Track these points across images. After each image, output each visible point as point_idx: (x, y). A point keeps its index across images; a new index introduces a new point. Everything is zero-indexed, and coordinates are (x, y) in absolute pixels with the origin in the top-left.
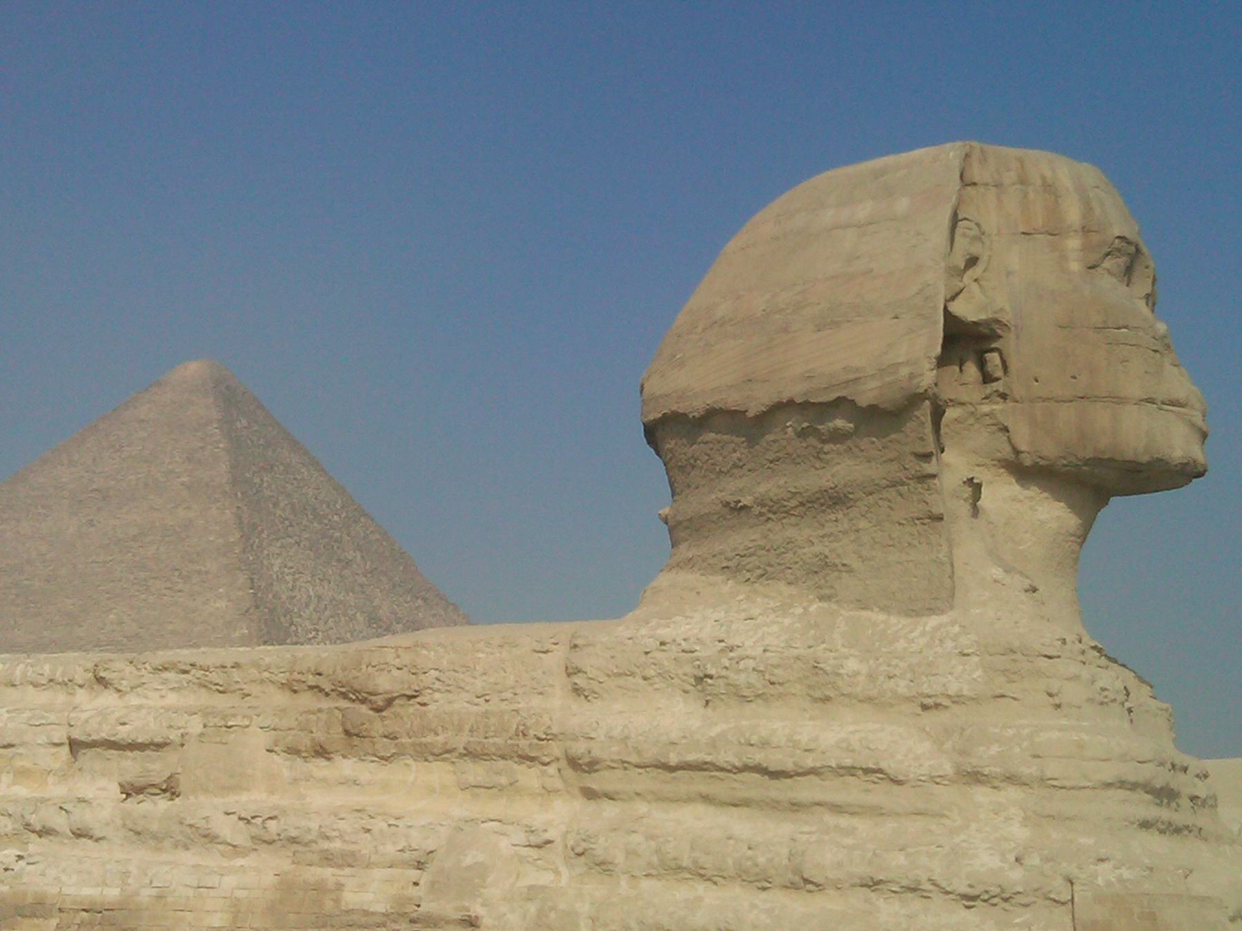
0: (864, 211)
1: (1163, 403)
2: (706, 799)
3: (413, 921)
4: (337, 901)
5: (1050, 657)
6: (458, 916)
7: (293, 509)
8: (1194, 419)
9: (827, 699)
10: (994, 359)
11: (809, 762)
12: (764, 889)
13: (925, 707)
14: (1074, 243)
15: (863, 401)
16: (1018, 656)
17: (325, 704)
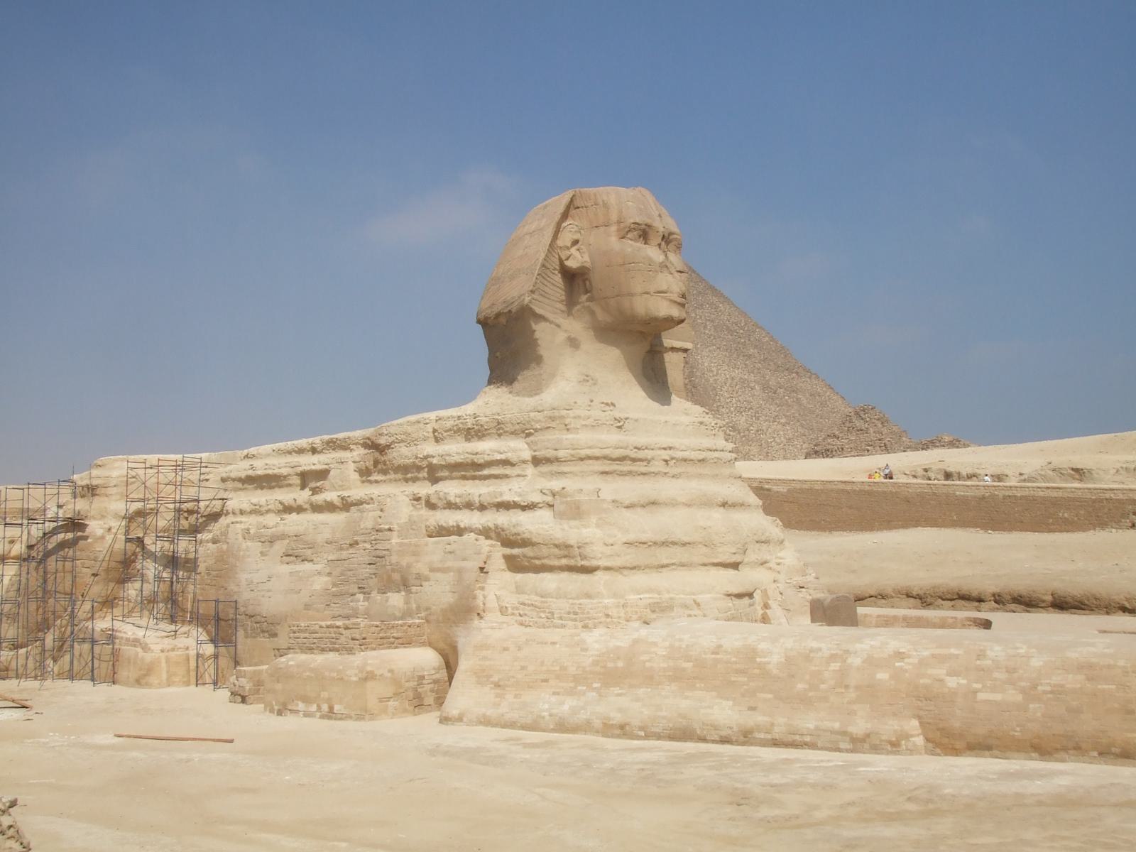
0: (533, 227)
1: (655, 293)
2: (464, 478)
3: (377, 531)
4: (359, 526)
5: (568, 410)
6: (387, 527)
7: (715, 328)
8: (671, 298)
9: (500, 435)
10: (588, 283)
11: (487, 458)
12: (472, 510)
13: (526, 434)
14: (614, 228)
15: (514, 311)
16: (554, 411)
17: (369, 451)
